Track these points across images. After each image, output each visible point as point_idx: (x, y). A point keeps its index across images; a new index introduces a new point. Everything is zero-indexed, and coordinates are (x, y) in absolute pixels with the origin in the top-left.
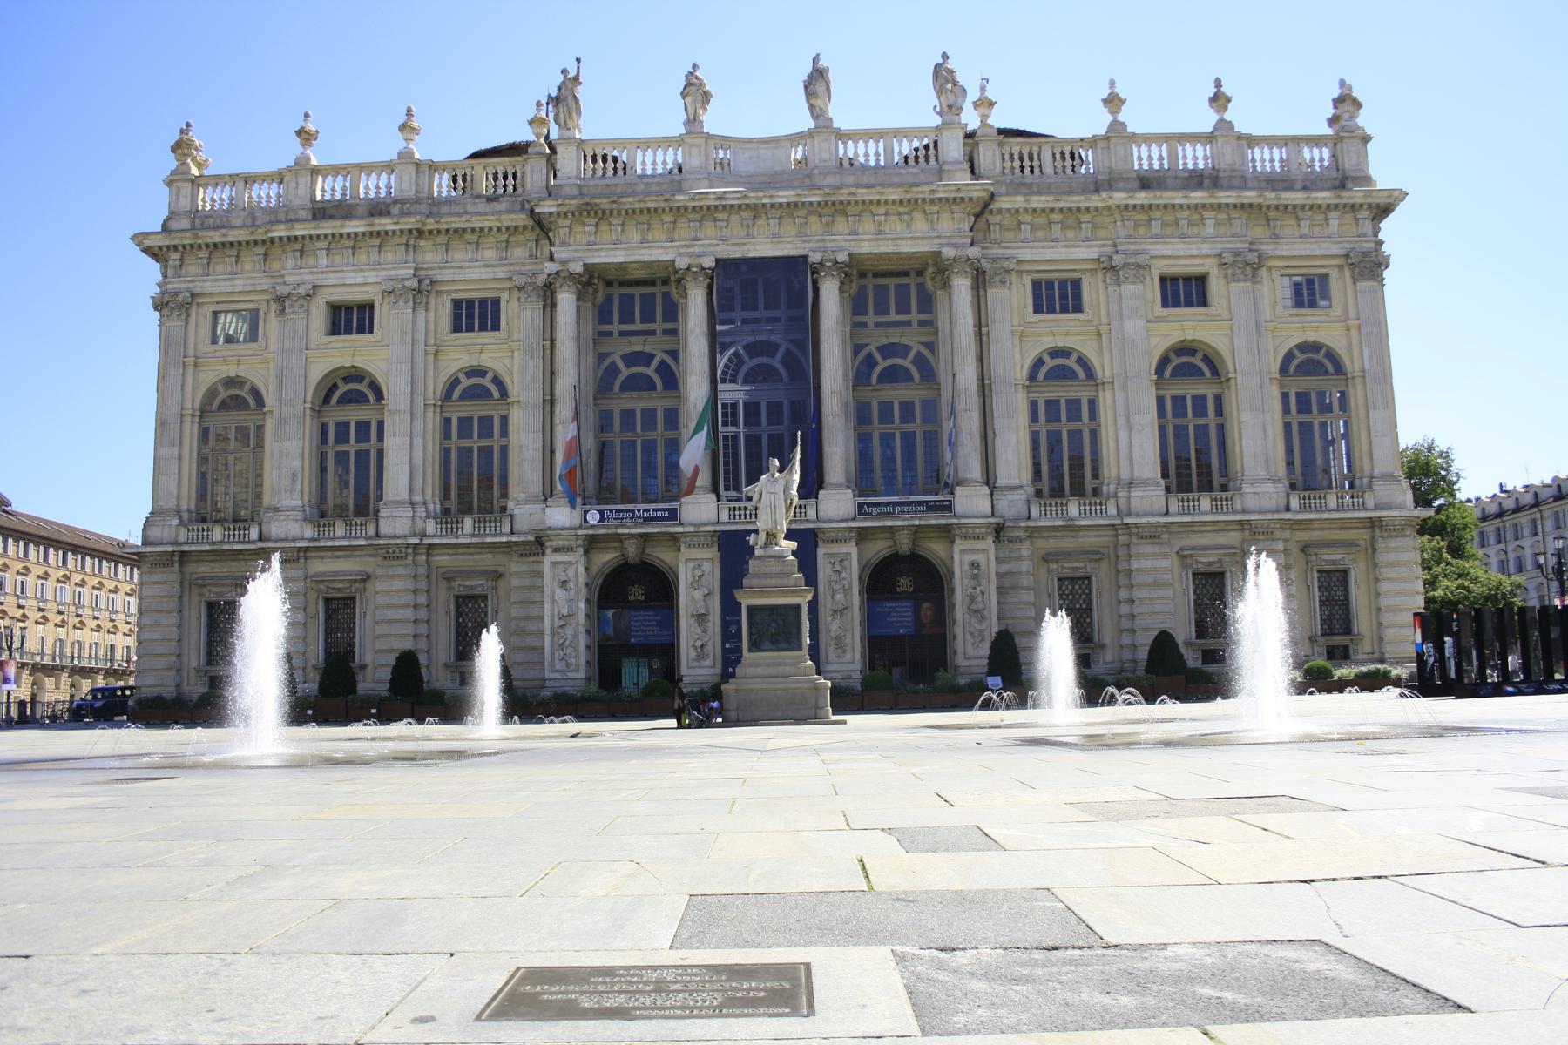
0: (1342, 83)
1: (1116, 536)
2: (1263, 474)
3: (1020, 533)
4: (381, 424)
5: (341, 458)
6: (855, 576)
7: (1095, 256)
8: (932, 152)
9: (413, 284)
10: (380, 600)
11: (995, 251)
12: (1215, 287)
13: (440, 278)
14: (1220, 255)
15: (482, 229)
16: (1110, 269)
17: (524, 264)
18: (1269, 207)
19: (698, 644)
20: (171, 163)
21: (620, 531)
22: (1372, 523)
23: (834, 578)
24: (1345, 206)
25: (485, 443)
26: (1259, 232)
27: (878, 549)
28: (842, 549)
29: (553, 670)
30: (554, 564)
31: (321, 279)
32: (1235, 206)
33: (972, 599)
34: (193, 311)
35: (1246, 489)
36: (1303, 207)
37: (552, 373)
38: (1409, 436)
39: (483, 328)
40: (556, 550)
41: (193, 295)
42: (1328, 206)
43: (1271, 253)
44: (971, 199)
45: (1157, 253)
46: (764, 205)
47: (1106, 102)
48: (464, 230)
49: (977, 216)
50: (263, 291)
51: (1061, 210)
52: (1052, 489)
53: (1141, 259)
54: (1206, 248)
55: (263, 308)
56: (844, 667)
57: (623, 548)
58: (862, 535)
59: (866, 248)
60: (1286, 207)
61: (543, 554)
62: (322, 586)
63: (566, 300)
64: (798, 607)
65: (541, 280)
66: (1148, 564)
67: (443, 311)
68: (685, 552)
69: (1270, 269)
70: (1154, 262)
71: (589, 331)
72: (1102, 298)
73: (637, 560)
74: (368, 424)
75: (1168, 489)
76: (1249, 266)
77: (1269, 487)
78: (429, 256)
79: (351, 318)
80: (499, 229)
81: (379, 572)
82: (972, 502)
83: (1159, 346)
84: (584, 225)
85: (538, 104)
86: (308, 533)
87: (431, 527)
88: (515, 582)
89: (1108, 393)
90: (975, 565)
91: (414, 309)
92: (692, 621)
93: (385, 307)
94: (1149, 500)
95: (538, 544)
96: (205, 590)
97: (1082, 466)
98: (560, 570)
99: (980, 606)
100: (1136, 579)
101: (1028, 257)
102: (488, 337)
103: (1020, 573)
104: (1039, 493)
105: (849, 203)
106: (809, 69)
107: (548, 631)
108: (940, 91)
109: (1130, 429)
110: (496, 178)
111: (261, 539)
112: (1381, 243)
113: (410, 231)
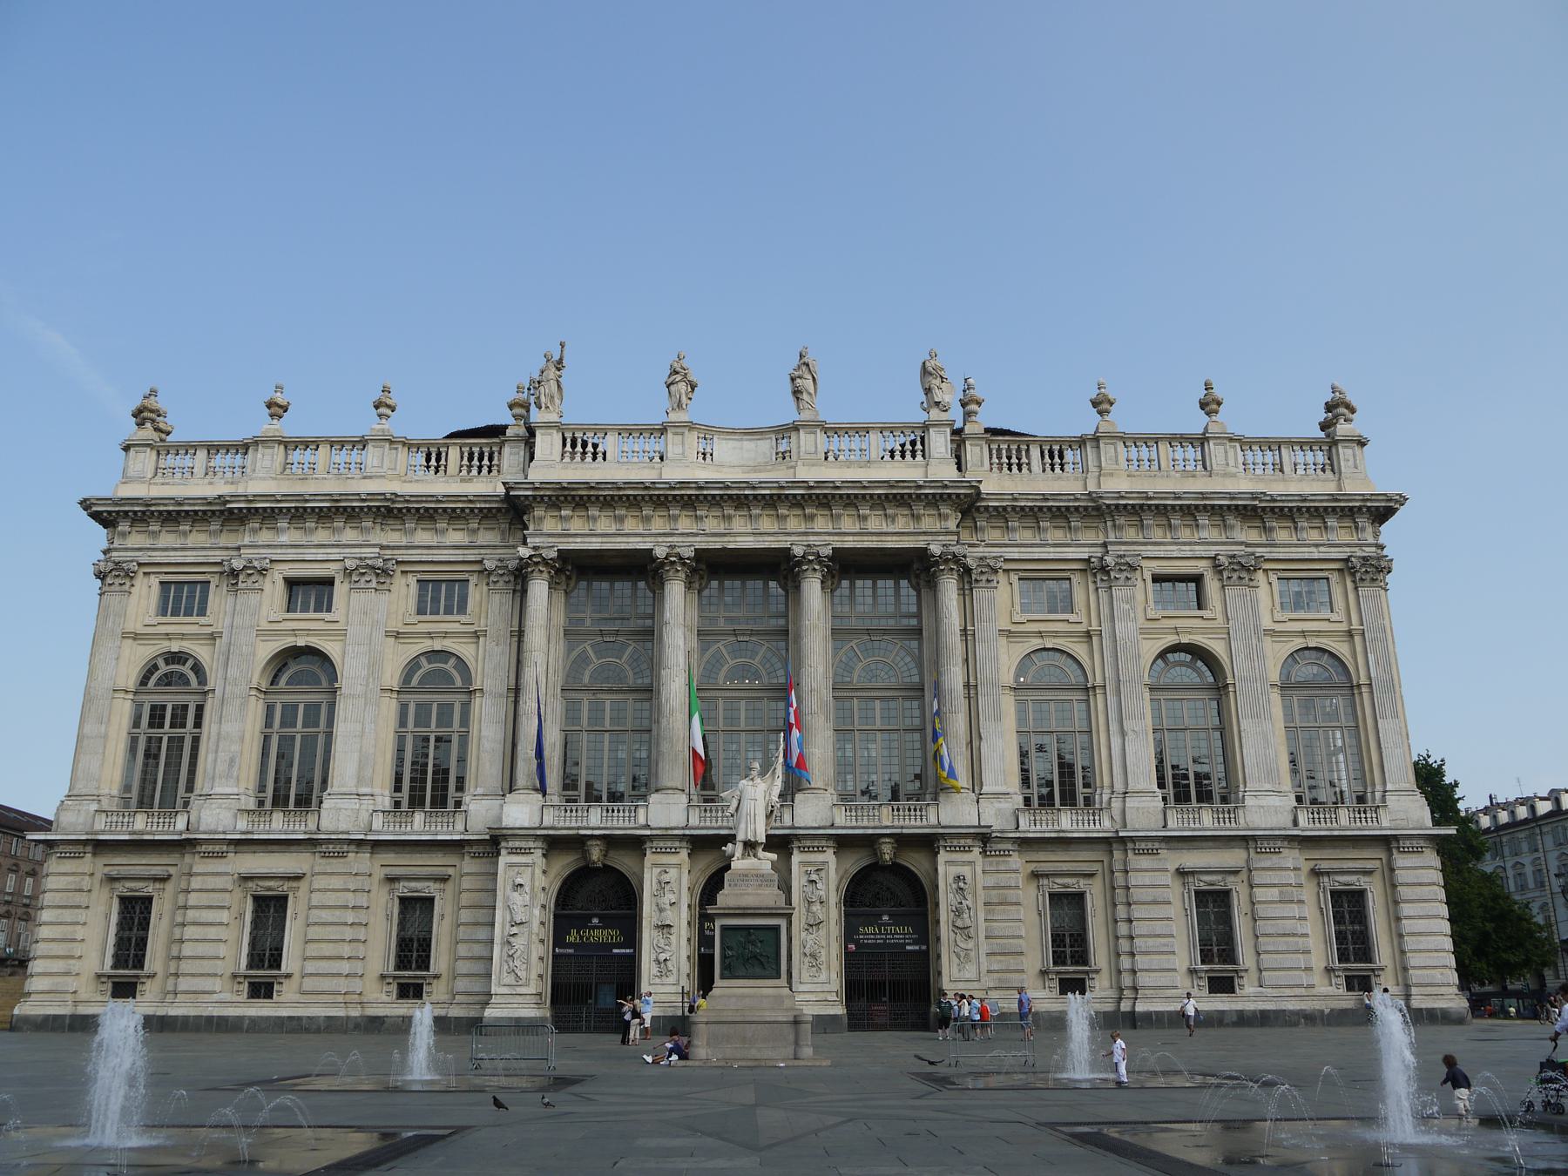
0: (1334, 389)
1: (1111, 852)
4: (332, 706)
5: (287, 741)
6: (833, 887)
7: (1086, 556)
8: (919, 446)
10: (316, 899)
11: (980, 551)
12: (1212, 585)
13: (406, 558)
14: (1214, 558)
15: (454, 510)
16: (1097, 570)
17: (495, 547)
18: (1264, 509)
19: (662, 957)
20: (129, 429)
21: (582, 832)
22: (1387, 842)
23: (809, 889)
24: (1342, 508)
25: (443, 731)
26: (1253, 536)
27: (856, 862)
28: (819, 857)
29: (500, 985)
30: (511, 865)
31: (277, 554)
32: (1229, 506)
33: (958, 913)
34: (140, 581)
35: (1249, 801)
36: (1299, 509)
37: (519, 662)
38: (1418, 751)
39: (448, 611)
40: (514, 851)
41: (140, 565)
42: (1326, 508)
43: (1267, 556)
44: (958, 495)
46: (746, 496)
47: (1095, 404)
48: (436, 510)
49: (963, 514)
50: (220, 564)
51: (1050, 508)
52: (1041, 798)
54: (1200, 550)
55: (214, 581)
56: (819, 988)
57: (585, 854)
58: (844, 843)
59: (849, 543)
60: (1282, 509)
61: (499, 854)
62: (250, 884)
63: (539, 589)
64: (777, 929)
65: (512, 564)
66: (1146, 879)
67: (404, 590)
68: (650, 858)
70: (1144, 563)
71: (559, 618)
72: (1092, 598)
73: (600, 865)
74: (317, 706)
75: (1164, 799)
76: (1240, 570)
77: (1274, 801)
79: (310, 591)
80: (472, 510)
81: (317, 869)
84: (560, 509)
85: (519, 389)
86: (242, 824)
87: (378, 822)
88: (466, 883)
89: (1100, 698)
90: (958, 878)
92: (655, 933)
93: (346, 586)
94: (1145, 809)
95: (494, 843)
96: (119, 886)
97: (1072, 774)
98: (512, 872)
99: (968, 923)
100: (1136, 894)
101: (1016, 556)
102: (452, 623)
103: (1009, 887)
104: (1027, 801)
105: (833, 495)
106: (796, 361)
107: (497, 940)
108: (928, 391)
109: (1123, 734)
110: (471, 459)
112: (1382, 547)
113: (378, 508)
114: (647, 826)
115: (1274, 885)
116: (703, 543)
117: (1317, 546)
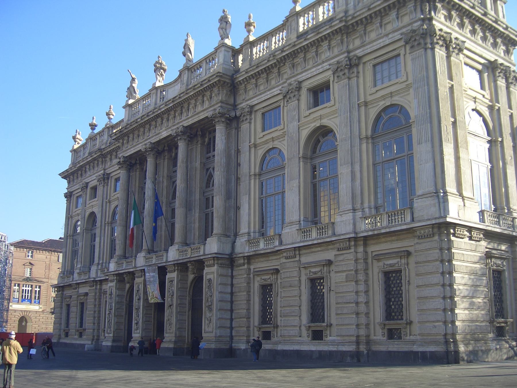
2: (350, 207)
3: (242, 261)
9: (102, 176)
11: (243, 105)
18: (352, 24)
26: (357, 42)
30: (110, 287)
31: (87, 180)
32: (332, 32)
40: (112, 281)
43: (360, 55)
45: (304, 78)
53: (295, 85)
54: (326, 65)
59: (190, 122)
60: (361, 20)
69: (364, 63)
77: (349, 216)
78: (109, 164)
82: (212, 246)
83: (305, 133)
90: (210, 280)
91: (104, 186)
101: (256, 102)
111: (73, 281)
114: (135, 267)
115: (344, 271)
116: (154, 140)
117: (387, 35)
